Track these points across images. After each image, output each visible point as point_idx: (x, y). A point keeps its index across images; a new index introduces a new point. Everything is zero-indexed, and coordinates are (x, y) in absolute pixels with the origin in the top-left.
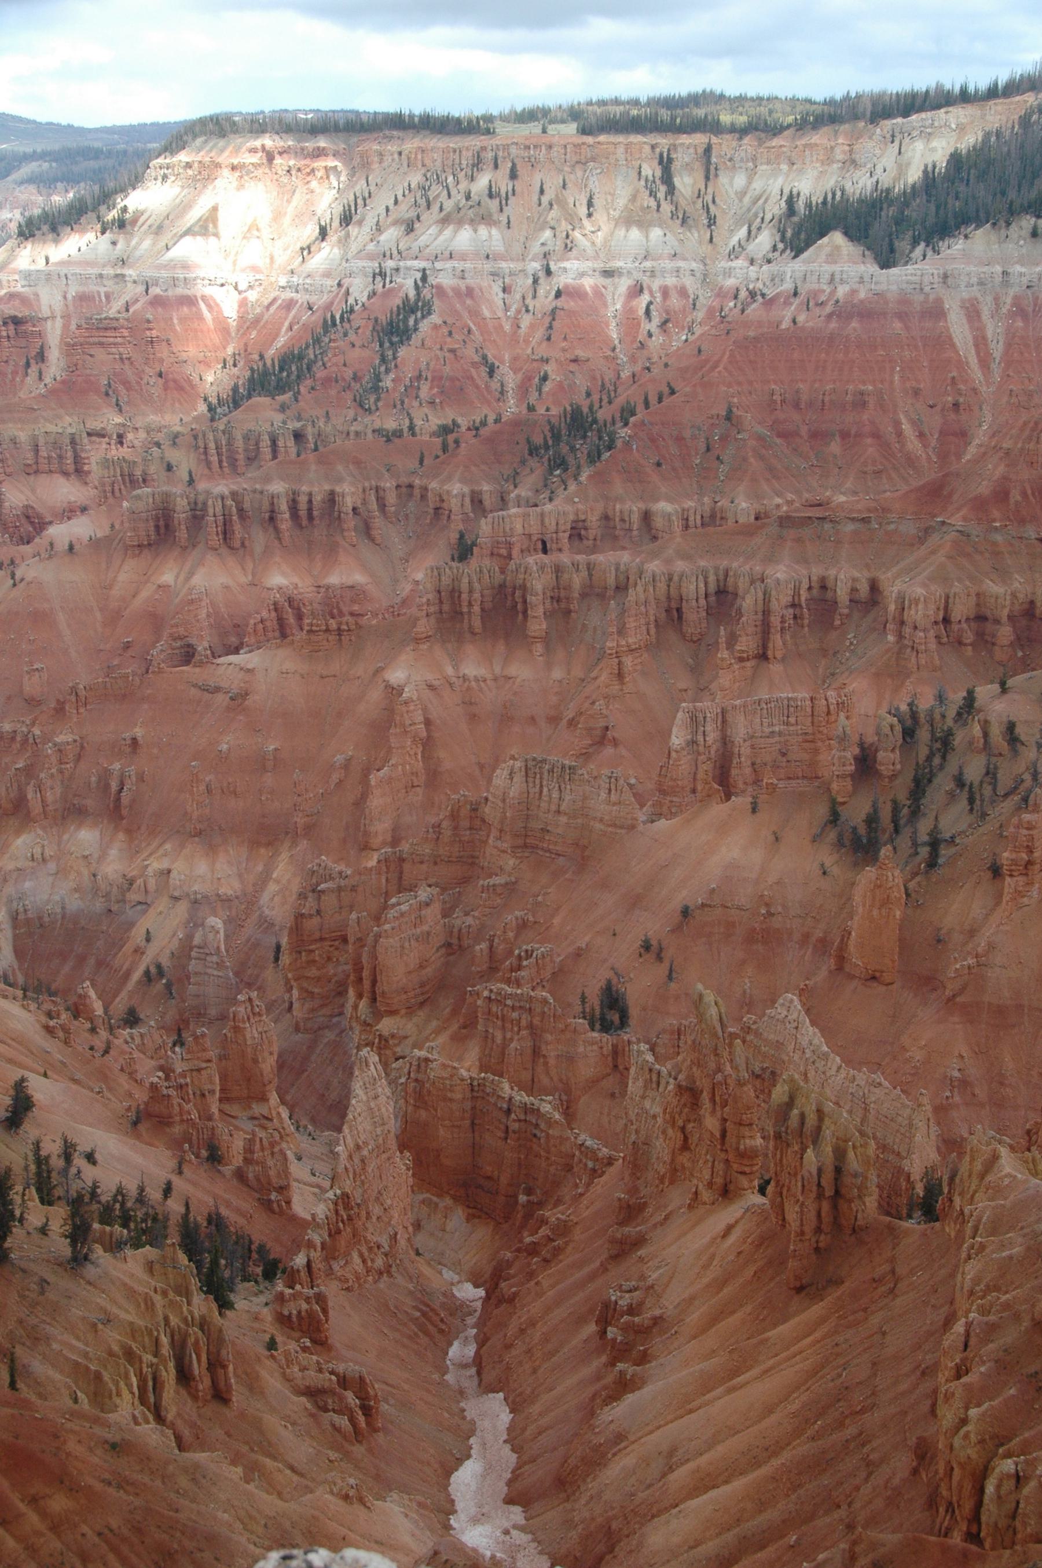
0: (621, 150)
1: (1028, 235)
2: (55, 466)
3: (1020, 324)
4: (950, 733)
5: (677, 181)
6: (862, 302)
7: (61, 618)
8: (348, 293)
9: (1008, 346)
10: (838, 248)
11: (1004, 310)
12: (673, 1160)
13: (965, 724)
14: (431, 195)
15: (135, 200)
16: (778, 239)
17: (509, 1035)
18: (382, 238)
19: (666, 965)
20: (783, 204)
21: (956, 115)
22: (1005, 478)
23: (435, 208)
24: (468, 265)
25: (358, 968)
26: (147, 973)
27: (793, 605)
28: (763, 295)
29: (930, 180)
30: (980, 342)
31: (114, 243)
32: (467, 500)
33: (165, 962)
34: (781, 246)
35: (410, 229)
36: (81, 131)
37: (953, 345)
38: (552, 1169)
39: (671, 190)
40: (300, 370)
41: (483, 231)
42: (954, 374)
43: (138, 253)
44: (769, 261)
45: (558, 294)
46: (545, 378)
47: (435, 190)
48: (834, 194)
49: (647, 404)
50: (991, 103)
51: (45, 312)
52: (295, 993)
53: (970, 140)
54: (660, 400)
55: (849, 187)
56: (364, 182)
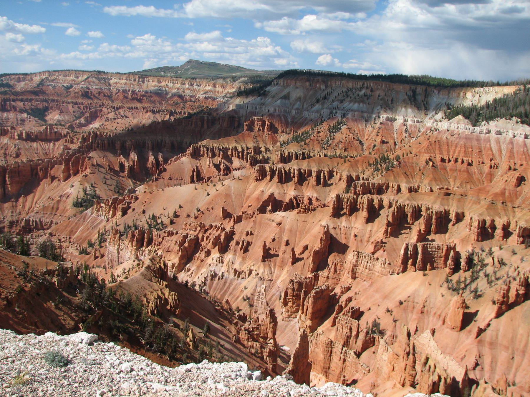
0: (401, 87)
1: (515, 122)
2: (237, 155)
3: (511, 146)
4: (483, 260)
5: (417, 97)
6: (466, 135)
7: (233, 197)
8: (322, 117)
9: (507, 151)
11: (507, 142)
12: (389, 374)
13: (488, 258)
14: (348, 94)
15: (268, 89)
16: (444, 115)
17: (344, 330)
18: (334, 104)
19: (392, 317)
21: (496, 88)
22: (505, 189)
23: (349, 98)
24: (356, 113)
25: (303, 305)
26: (244, 297)
27: (440, 218)
29: (488, 105)
30: (500, 151)
31: (262, 99)
32: (349, 178)
33: (249, 295)
34: (444, 117)
35: (342, 102)
36: (257, 71)
37: (492, 150)
38: (352, 371)
39: (415, 100)
40: (306, 136)
41: (361, 105)
42: (491, 157)
43: (267, 103)
44: (441, 121)
45: (381, 123)
46: (375, 146)
47: (350, 93)
49: (403, 156)
51: (241, 115)
52: (284, 309)
53: (499, 96)
54: (407, 155)
56: (330, 89)
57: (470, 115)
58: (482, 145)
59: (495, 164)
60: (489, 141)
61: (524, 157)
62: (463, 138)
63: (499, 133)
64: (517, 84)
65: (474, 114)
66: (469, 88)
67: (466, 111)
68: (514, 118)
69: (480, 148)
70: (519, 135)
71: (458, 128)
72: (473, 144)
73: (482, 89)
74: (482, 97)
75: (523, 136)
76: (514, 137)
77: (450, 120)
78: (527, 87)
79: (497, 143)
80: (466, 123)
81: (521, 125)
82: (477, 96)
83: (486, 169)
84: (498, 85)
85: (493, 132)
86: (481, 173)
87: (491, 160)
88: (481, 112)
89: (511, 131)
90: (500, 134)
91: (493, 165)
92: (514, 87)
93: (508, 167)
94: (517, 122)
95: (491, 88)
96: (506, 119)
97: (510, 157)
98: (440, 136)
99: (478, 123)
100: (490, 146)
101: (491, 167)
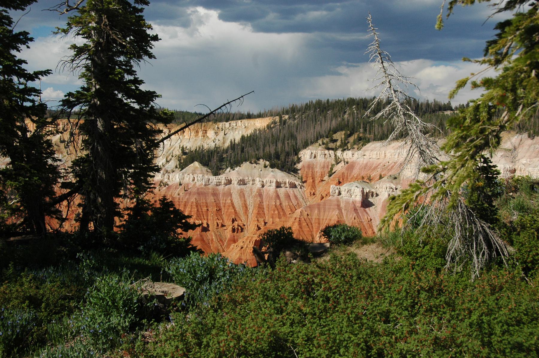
3: (259, 199)
6: (198, 189)
9: (254, 207)
10: (197, 167)
11: (254, 194)
16: (178, 163)
20: (180, 151)
21: (246, 122)
28: (168, 184)
29: (233, 146)
34: (178, 167)
37: (234, 207)
44: (173, 171)
48: (199, 148)
50: (258, 119)
55: (206, 147)
57: (210, 160)
58: (221, 202)
59: (238, 226)
60: (229, 194)
61: (276, 212)
62: (194, 194)
63: (242, 182)
64: (271, 115)
65: (215, 159)
66: (211, 123)
67: (204, 155)
68: (261, 160)
69: (218, 205)
70: (268, 184)
71: (194, 180)
72: (208, 201)
73: (227, 124)
74: (227, 135)
75: (274, 184)
76: (263, 186)
77: (182, 169)
78: (283, 119)
79: (240, 195)
80: (205, 172)
81: (271, 169)
82: (221, 134)
83: (228, 233)
84: (249, 116)
85: (235, 182)
86: (221, 240)
87: (233, 221)
88: (225, 156)
89: (258, 179)
90: (246, 184)
91: (236, 227)
92: (268, 118)
93: (256, 228)
94: (265, 167)
95: (239, 121)
96: (251, 163)
97: (258, 214)
98: (170, 193)
99: (221, 171)
100: (232, 201)
101: (233, 230)
